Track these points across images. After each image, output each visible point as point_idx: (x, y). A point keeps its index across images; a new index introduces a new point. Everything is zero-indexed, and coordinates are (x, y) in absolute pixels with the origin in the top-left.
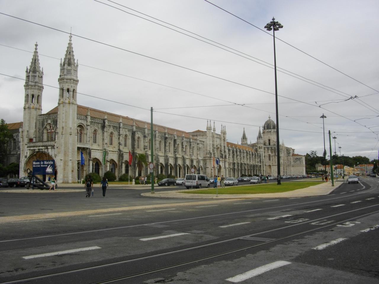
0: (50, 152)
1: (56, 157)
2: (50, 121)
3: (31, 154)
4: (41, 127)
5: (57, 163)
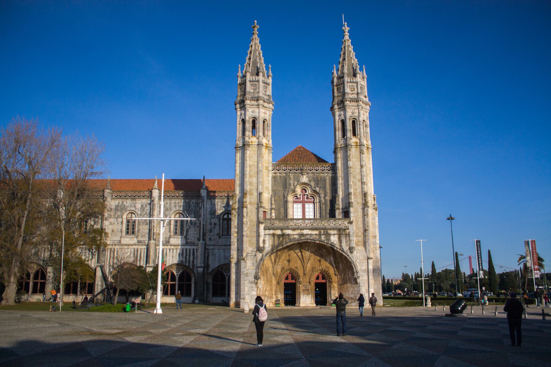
0: (335, 243)
1: (351, 252)
2: (307, 179)
3: (276, 243)
5: (358, 264)
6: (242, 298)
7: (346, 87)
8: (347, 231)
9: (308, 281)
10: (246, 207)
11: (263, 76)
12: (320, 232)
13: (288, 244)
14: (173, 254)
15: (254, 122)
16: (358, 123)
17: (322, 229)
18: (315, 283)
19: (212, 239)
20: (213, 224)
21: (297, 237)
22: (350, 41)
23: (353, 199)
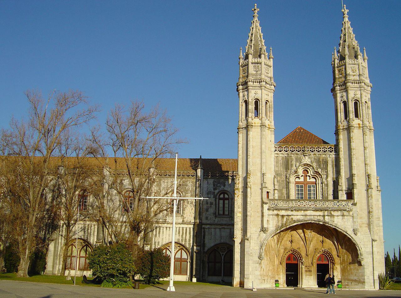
2: (310, 160)
4: (282, 169)
6: (246, 278)
7: (347, 69)
8: (351, 213)
9: (310, 262)
10: (251, 188)
11: (265, 58)
12: (324, 213)
13: (291, 225)
14: (169, 232)
15: (257, 103)
16: (361, 105)
17: (326, 210)
18: (317, 264)
19: (209, 218)
20: (209, 203)
21: (301, 218)
22: (350, 23)
23: (356, 181)
